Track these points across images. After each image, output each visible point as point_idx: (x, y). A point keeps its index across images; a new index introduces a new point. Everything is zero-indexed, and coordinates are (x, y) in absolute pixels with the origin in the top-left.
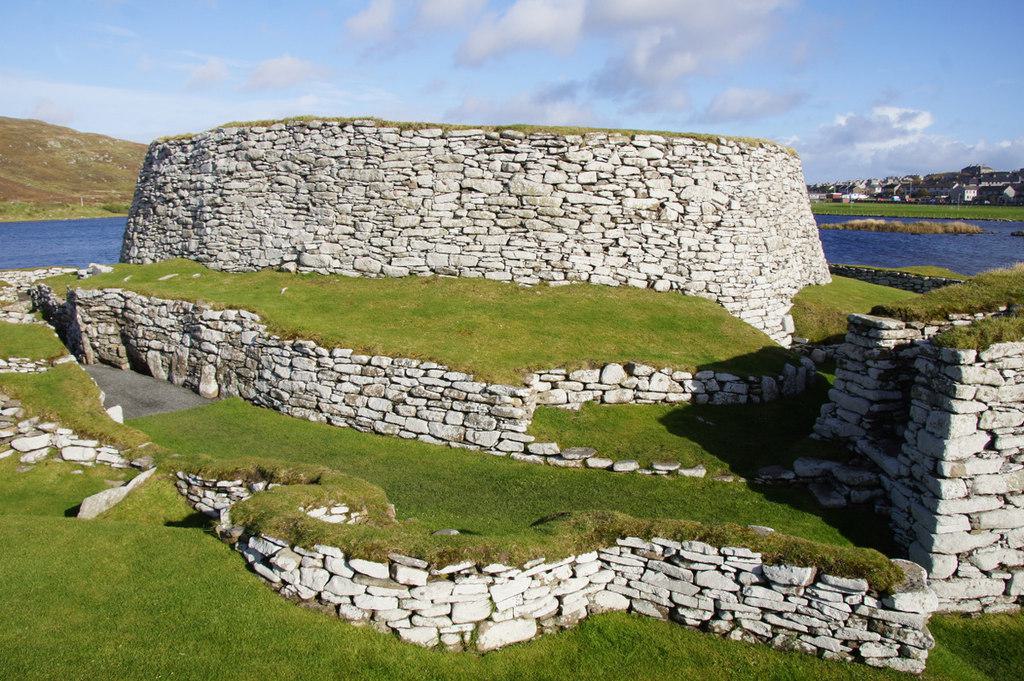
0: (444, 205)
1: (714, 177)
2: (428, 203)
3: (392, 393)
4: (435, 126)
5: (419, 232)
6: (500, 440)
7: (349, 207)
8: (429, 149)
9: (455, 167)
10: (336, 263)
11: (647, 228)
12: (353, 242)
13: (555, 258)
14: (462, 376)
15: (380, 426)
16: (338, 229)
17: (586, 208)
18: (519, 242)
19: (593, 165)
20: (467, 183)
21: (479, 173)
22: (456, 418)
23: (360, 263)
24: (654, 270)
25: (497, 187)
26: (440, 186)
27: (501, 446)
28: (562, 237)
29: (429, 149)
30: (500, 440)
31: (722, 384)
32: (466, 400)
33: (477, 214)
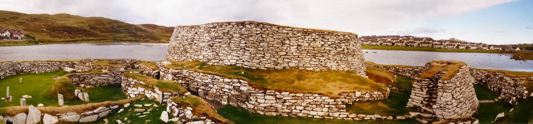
0: (293, 49)
1: (353, 43)
2: (288, 49)
3: (303, 104)
4: (289, 27)
5: (287, 57)
6: (340, 115)
7: (262, 49)
8: (288, 33)
9: (295, 39)
10: (258, 66)
11: (342, 56)
12: (264, 59)
13: (323, 64)
14: (327, 98)
15: (301, 115)
16: (260, 55)
17: (330, 50)
18: (313, 59)
19: (330, 40)
20: (300, 43)
21: (302, 41)
22: (325, 110)
23: (267, 66)
24: (344, 66)
25: (307, 45)
26: (291, 44)
27: (340, 116)
28: (324, 58)
29: (288, 33)
30: (340, 115)
31: (379, 95)
32: (329, 104)
33: (302, 52)
